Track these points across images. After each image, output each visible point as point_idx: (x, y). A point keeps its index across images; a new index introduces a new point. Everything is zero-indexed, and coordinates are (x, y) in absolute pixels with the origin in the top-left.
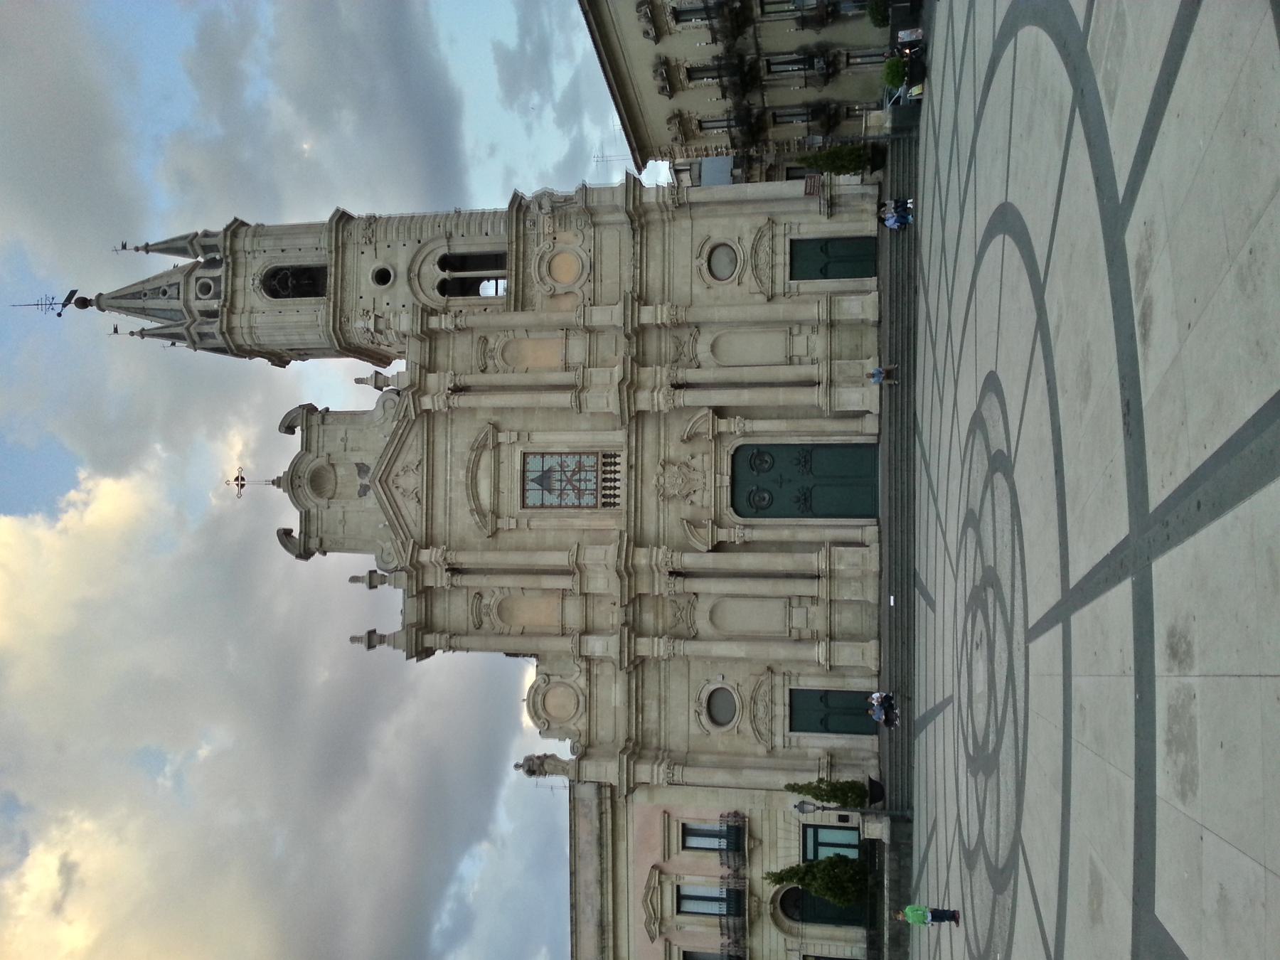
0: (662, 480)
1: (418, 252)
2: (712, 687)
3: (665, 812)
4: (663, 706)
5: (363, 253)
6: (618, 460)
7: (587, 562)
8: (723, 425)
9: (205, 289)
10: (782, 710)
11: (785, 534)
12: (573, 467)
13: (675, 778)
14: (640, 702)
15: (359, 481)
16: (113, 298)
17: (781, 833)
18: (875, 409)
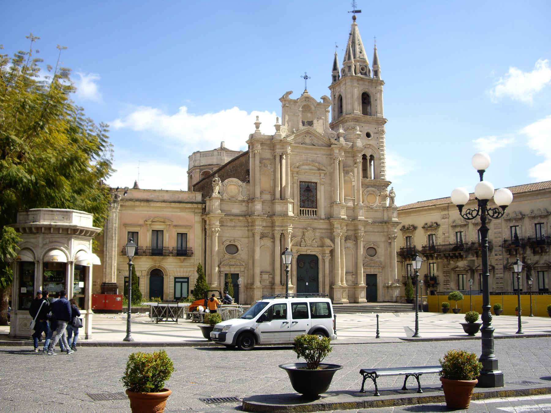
15: (306, 121)
17: (185, 269)
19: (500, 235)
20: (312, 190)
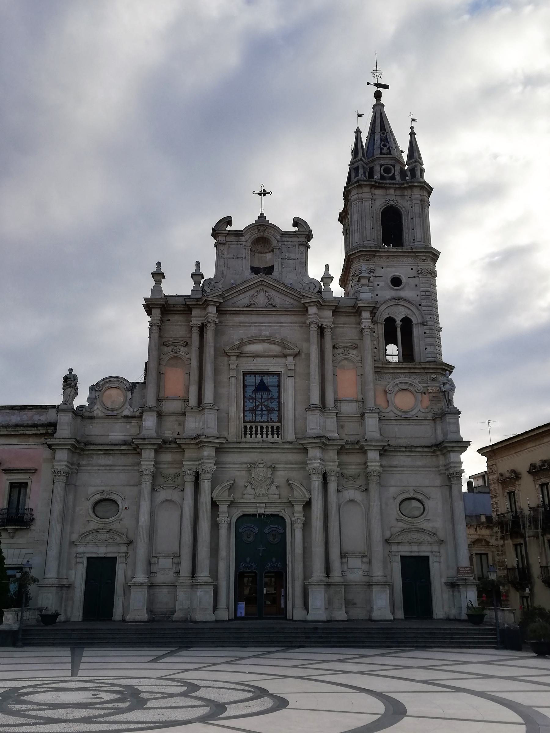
0: (261, 466)
1: (414, 305)
2: (119, 503)
3: (36, 470)
4: (108, 468)
5: (412, 269)
6: (275, 436)
7: (206, 416)
8: (299, 508)
9: (387, 170)
10: (102, 551)
11: (223, 553)
12: (271, 406)
13: (57, 477)
14: (111, 452)
16: (381, 114)
17: (17, 552)
18: (309, 618)
20: (270, 388)
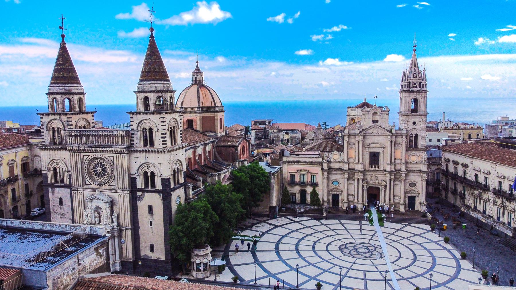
19: (493, 184)
